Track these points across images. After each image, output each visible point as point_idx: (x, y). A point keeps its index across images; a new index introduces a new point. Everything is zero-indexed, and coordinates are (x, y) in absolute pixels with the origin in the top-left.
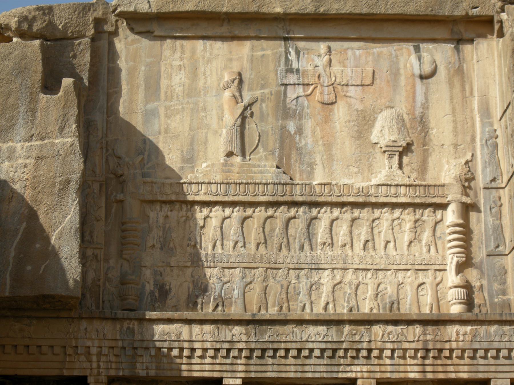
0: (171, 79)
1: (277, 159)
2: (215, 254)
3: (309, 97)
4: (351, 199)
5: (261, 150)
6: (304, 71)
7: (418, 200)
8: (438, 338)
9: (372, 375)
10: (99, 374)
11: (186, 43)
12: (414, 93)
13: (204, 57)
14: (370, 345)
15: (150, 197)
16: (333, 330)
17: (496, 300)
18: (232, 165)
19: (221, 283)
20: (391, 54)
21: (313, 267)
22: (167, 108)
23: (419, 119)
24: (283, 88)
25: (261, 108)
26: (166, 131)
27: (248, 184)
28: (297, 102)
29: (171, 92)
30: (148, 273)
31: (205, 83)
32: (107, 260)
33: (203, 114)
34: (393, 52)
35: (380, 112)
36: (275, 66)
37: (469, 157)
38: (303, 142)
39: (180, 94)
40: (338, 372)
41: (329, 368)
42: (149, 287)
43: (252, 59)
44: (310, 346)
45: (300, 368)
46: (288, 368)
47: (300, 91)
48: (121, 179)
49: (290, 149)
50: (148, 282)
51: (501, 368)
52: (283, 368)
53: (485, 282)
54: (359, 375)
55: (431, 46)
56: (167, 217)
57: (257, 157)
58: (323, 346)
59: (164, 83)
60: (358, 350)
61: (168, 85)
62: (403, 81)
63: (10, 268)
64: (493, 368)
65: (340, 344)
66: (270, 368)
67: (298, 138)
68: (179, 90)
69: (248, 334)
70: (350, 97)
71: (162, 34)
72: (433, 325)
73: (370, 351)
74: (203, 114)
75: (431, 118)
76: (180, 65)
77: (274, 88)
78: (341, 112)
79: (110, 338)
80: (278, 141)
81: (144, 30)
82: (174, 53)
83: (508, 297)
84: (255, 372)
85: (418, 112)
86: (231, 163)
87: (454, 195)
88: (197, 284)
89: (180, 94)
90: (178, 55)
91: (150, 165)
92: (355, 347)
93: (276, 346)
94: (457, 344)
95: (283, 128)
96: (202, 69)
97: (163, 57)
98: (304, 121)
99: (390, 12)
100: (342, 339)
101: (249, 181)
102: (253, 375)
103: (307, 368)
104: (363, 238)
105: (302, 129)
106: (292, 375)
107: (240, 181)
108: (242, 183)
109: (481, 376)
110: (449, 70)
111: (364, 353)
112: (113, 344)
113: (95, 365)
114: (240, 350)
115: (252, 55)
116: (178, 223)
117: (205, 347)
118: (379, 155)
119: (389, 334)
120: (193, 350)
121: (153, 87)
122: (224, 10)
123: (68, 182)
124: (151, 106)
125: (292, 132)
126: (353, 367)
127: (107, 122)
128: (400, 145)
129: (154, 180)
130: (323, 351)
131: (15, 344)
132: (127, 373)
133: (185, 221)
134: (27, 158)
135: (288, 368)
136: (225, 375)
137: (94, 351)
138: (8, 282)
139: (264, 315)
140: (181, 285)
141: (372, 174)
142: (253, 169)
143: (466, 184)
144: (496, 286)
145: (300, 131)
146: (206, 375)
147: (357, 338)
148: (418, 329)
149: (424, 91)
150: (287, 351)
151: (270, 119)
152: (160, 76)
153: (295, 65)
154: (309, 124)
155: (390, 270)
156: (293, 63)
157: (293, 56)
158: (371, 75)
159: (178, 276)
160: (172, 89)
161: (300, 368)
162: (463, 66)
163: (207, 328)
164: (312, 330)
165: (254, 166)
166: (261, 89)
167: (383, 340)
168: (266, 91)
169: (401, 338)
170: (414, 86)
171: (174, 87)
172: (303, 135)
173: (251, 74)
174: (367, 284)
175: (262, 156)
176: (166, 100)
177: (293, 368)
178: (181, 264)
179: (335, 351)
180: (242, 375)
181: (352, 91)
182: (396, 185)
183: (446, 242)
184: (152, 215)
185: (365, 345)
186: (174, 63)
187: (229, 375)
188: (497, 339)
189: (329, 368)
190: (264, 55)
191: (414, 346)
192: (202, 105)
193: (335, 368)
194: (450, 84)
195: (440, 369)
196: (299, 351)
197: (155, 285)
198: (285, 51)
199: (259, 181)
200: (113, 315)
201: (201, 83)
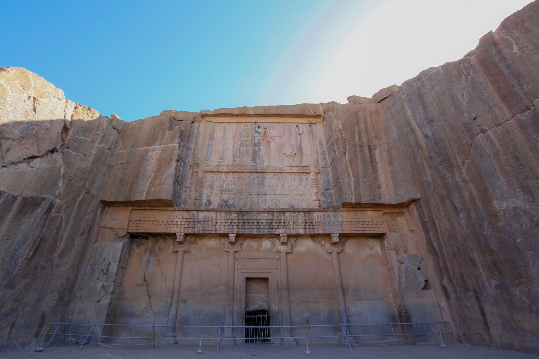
4: (277, 171)
7: (300, 171)
10: (181, 232)
11: (223, 124)
30: (204, 196)
32: (190, 192)
37: (316, 158)
42: (205, 201)
43: (244, 129)
44: (262, 221)
47: (260, 138)
51: (335, 229)
52: (251, 230)
55: (302, 125)
59: (215, 136)
62: (293, 135)
64: (332, 230)
69: (238, 217)
73: (284, 223)
77: (251, 137)
78: (273, 145)
87: (312, 169)
102: (240, 233)
103: (261, 230)
104: (282, 184)
109: (327, 233)
111: (283, 224)
113: (179, 229)
118: (286, 158)
121: (212, 138)
132: (192, 232)
137: (179, 223)
144: (329, 200)
145: (259, 150)
146: (222, 232)
148: (302, 214)
150: (253, 223)
151: (250, 147)
153: (258, 131)
154: (263, 149)
161: (258, 230)
163: (223, 214)
180: (236, 232)
181: (276, 138)
184: (208, 176)
185: (283, 221)
188: (332, 218)
191: (301, 221)
193: (271, 230)
195: (312, 230)
196: (258, 223)
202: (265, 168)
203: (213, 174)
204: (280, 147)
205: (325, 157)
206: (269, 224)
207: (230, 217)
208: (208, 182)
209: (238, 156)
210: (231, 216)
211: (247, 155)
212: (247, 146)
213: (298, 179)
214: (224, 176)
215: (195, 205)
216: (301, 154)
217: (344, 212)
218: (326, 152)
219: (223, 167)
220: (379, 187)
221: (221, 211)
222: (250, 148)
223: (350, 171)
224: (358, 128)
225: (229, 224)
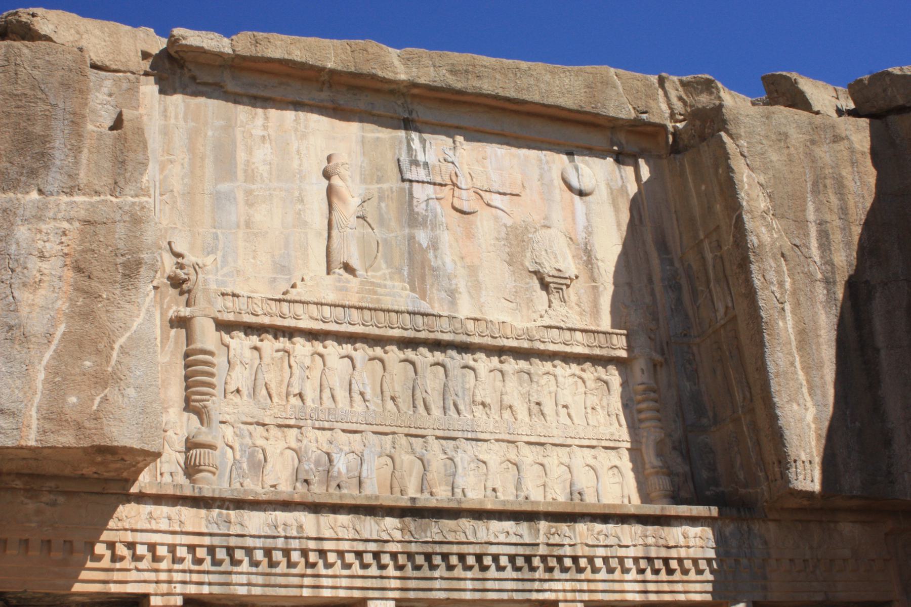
0: (251, 154)
1: (407, 280)
2: (329, 409)
3: (442, 201)
5: (384, 266)
6: (434, 166)
7: (597, 352)
8: (661, 542)
9: (578, 596)
12: (573, 213)
13: (296, 130)
14: (574, 551)
15: (231, 317)
16: (524, 528)
17: (708, 493)
18: (348, 281)
19: (343, 454)
20: (540, 160)
21: (469, 436)
22: (249, 193)
23: (583, 246)
24: (407, 185)
25: (379, 208)
26: (248, 225)
27: (375, 310)
28: (427, 205)
29: (253, 170)
31: (300, 165)
33: (300, 207)
34: (543, 157)
35: (535, 232)
36: (395, 154)
38: (439, 262)
39: (265, 175)
40: (530, 591)
41: (520, 586)
43: (363, 142)
44: (494, 550)
45: (478, 585)
46: (462, 584)
47: (430, 190)
48: (185, 286)
49: (423, 268)
50: (231, 447)
53: (687, 468)
54: (561, 596)
56: (256, 348)
57: (379, 274)
58: (512, 550)
59: (241, 156)
60: (560, 559)
61: (248, 161)
63: (37, 398)
65: (535, 548)
66: (437, 584)
67: (431, 255)
68: (263, 169)
70: (496, 208)
71: (238, 90)
72: (653, 524)
74: (300, 207)
75: (597, 246)
76: (264, 136)
78: (485, 226)
79: (190, 529)
80: (406, 255)
81: (211, 81)
82: (253, 118)
83: (721, 489)
84: (414, 590)
85: (581, 236)
86: (347, 279)
88: (306, 452)
89: (265, 175)
90: (259, 121)
91: (225, 270)
92: (555, 554)
93: (445, 549)
94: (687, 552)
95: (411, 238)
96: (295, 146)
97: (239, 122)
98: (438, 232)
99: (545, 102)
100: (538, 541)
101: (376, 306)
102: (412, 595)
103: (489, 585)
105: (437, 243)
106: (468, 596)
107: (364, 305)
108: (366, 308)
110: (611, 189)
111: (568, 562)
112: (195, 540)
114: (394, 556)
115: (363, 136)
116: (273, 359)
117: (341, 548)
119: (598, 534)
120: (322, 553)
121: (226, 163)
122: (330, 65)
123: (139, 263)
124: (224, 187)
125: (425, 245)
126: (552, 583)
127: (161, 201)
128: (567, 276)
129: (237, 292)
130: (512, 558)
131: (26, 536)
133: (282, 358)
134: (70, 220)
135: (462, 584)
136: (371, 594)
137: (162, 551)
138: (34, 424)
139: (426, 501)
140: (282, 453)
141: (534, 312)
142: (379, 290)
143: (653, 336)
144: (705, 474)
145: (435, 245)
146: (342, 593)
147: (556, 540)
148: (638, 528)
149: (584, 211)
150: (462, 557)
151: (393, 224)
152: (236, 146)
153: (421, 157)
154: (445, 238)
155: (570, 446)
156: (418, 154)
157: (416, 145)
158: (519, 182)
159: (277, 439)
160: (253, 167)
161: (478, 585)
162: (626, 187)
164: (495, 525)
165: (380, 286)
166: (377, 183)
167: (591, 543)
168: (385, 186)
169: (612, 541)
170: (572, 202)
171: (256, 165)
172: (440, 251)
173: (363, 162)
174: (542, 465)
175: (384, 274)
176: (245, 181)
177: (469, 585)
178: (280, 422)
179: (528, 559)
182: (570, 329)
183: (635, 412)
185: (568, 551)
186: (254, 132)
187: (376, 594)
189: (520, 586)
190: (378, 138)
191: (631, 552)
192: (297, 194)
193: (528, 586)
194: (614, 206)
195: (666, 587)
197: (243, 451)
198: (407, 138)
199: (390, 307)
200: (196, 491)
201: (295, 164)
202: (470, 325)
203: (254, 339)
204: (517, 240)
205: (679, 301)
206: (520, 562)
207: (370, 527)
208: (238, 368)
209: (355, 263)
210: (375, 528)
211: (389, 263)
212: (382, 221)
213: (591, 384)
214: (302, 348)
215: (191, 470)
216: (594, 281)
217: (772, 526)
218: (684, 282)
219: (299, 309)
220: (888, 443)
221: (335, 509)
222: (397, 233)
223: (801, 375)
224: (817, 210)
225: (368, 558)
